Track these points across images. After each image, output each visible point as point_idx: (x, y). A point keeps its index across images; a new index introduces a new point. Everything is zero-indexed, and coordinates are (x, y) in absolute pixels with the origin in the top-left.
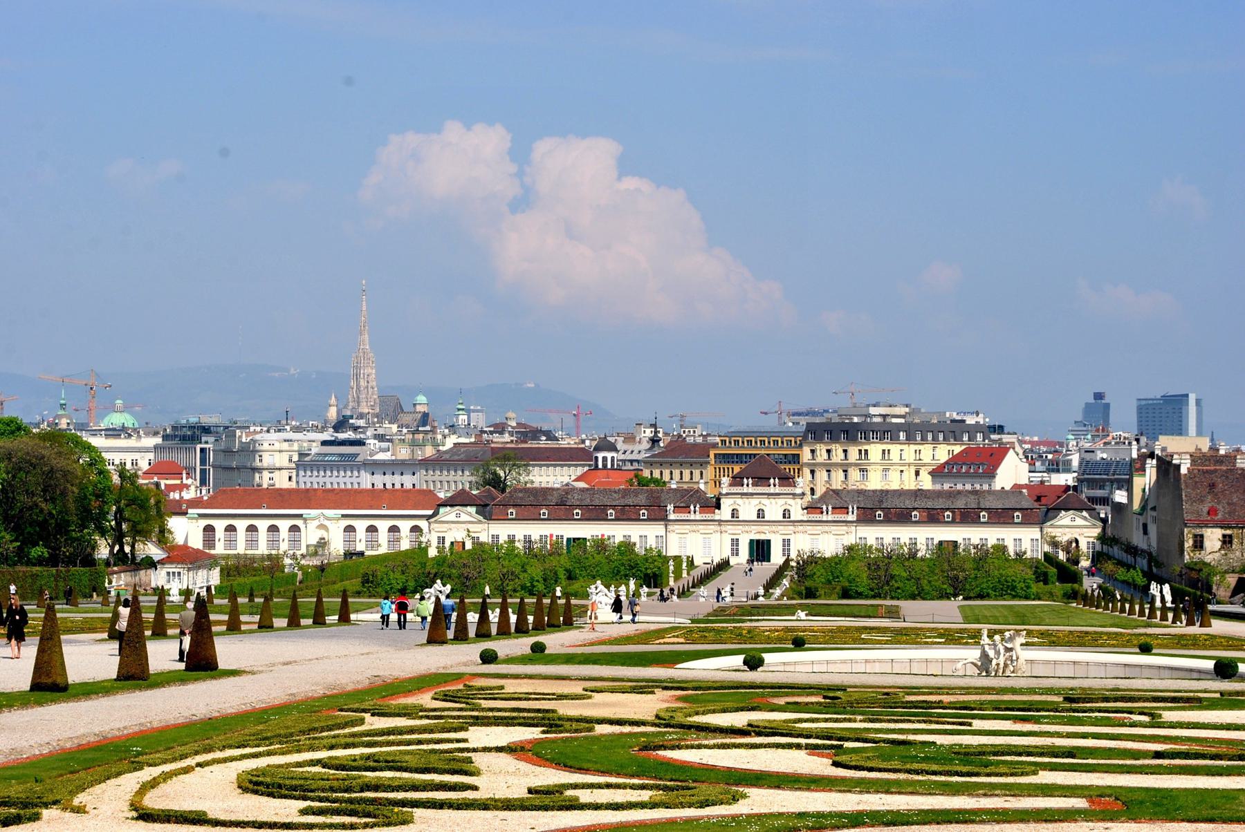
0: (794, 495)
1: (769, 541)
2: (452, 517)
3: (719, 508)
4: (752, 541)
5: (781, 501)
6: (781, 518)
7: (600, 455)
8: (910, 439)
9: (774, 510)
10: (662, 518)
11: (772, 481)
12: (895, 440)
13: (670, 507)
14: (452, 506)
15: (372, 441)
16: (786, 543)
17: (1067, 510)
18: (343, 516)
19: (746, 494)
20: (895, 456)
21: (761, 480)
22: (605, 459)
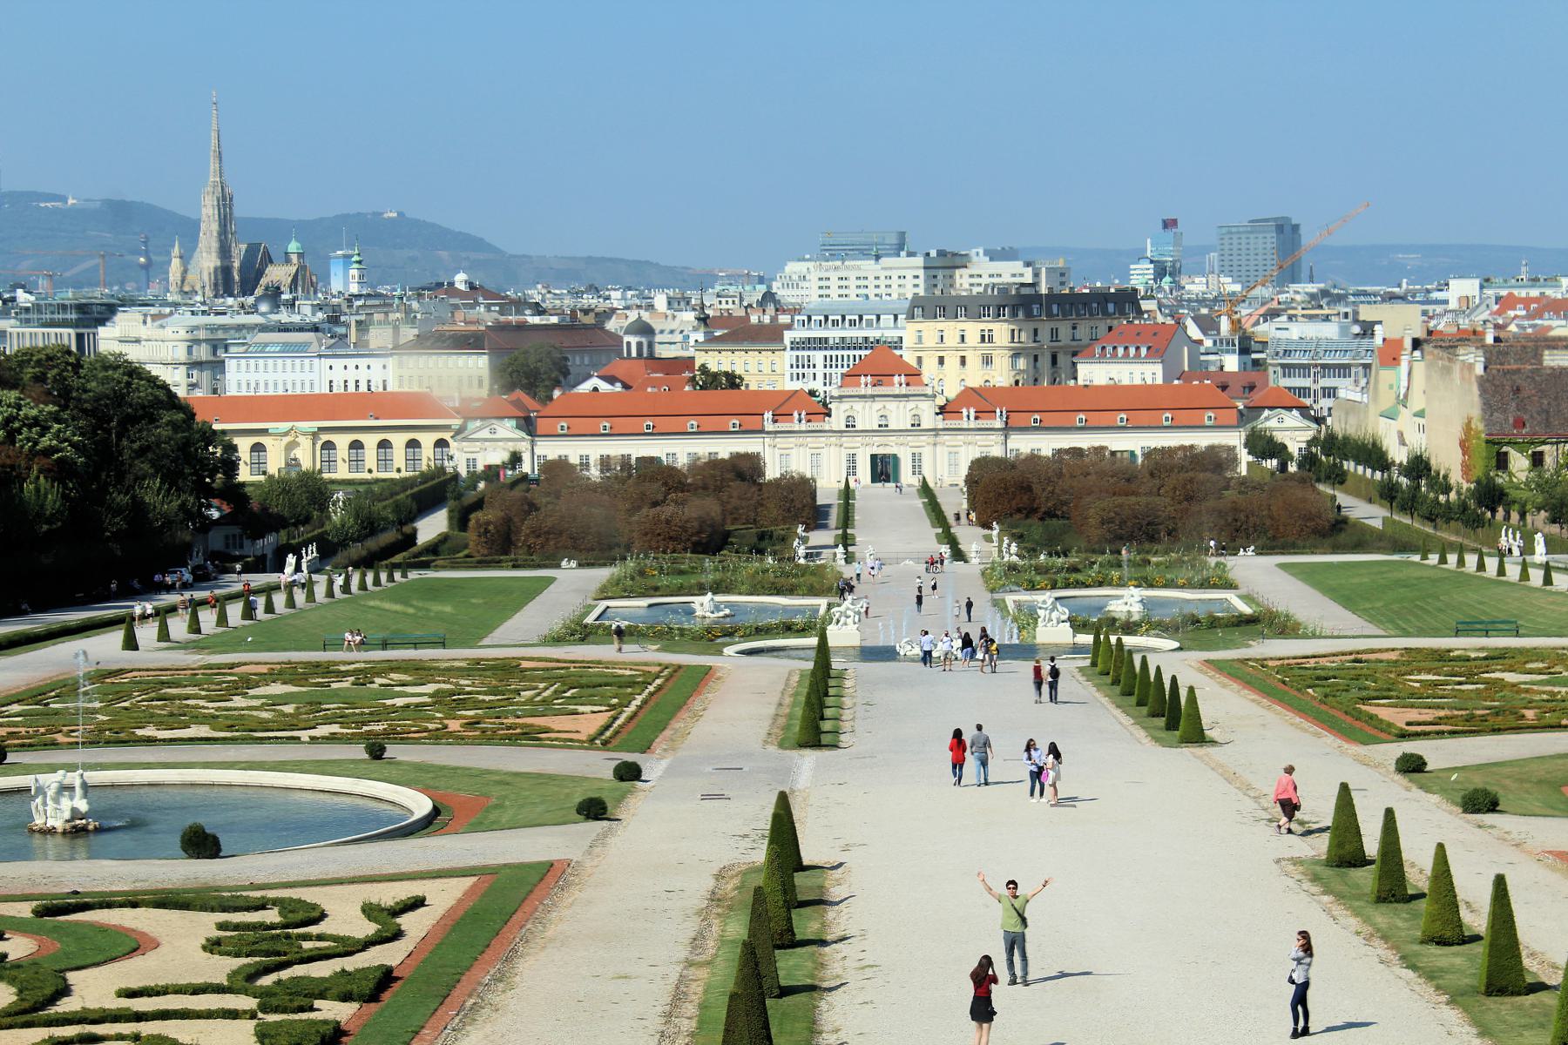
1: (895, 456)
2: (485, 434)
4: (874, 457)
5: (911, 405)
7: (633, 340)
9: (899, 415)
11: (896, 378)
13: (768, 415)
14: (483, 419)
15: (326, 326)
16: (916, 460)
17: (1271, 408)
18: (320, 429)
21: (881, 377)
22: (639, 345)
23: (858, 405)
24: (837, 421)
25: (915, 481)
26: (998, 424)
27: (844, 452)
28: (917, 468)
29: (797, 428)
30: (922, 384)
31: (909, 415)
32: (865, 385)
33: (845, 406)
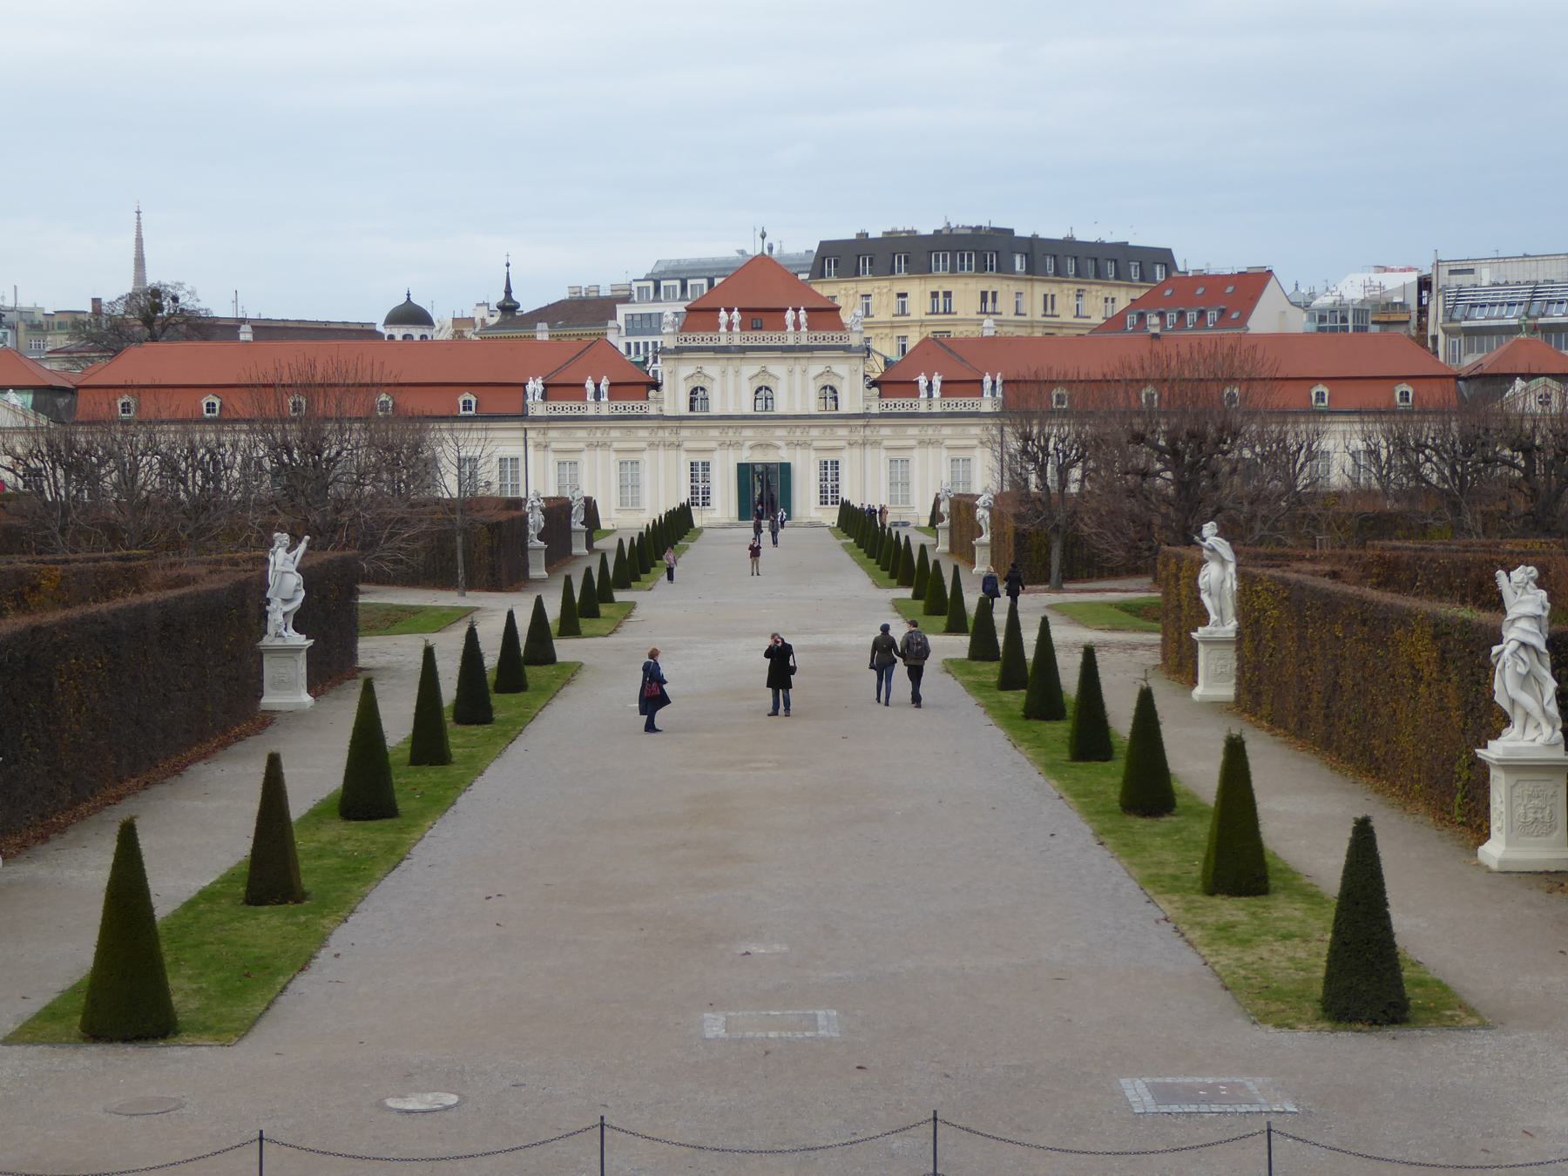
0: (847, 349)
1: (786, 469)
3: (656, 386)
4: (744, 470)
5: (816, 368)
6: (813, 407)
8: (1033, 270)
9: (796, 387)
10: (521, 416)
11: (790, 316)
12: (1004, 269)
13: (535, 386)
16: (830, 469)
17: (1528, 377)
19: (725, 350)
20: (1005, 306)
21: (761, 316)
23: (712, 369)
24: (673, 399)
25: (831, 516)
26: (987, 404)
27: (684, 460)
28: (829, 493)
29: (591, 412)
30: (840, 326)
31: (813, 391)
32: (729, 327)
33: (686, 369)
